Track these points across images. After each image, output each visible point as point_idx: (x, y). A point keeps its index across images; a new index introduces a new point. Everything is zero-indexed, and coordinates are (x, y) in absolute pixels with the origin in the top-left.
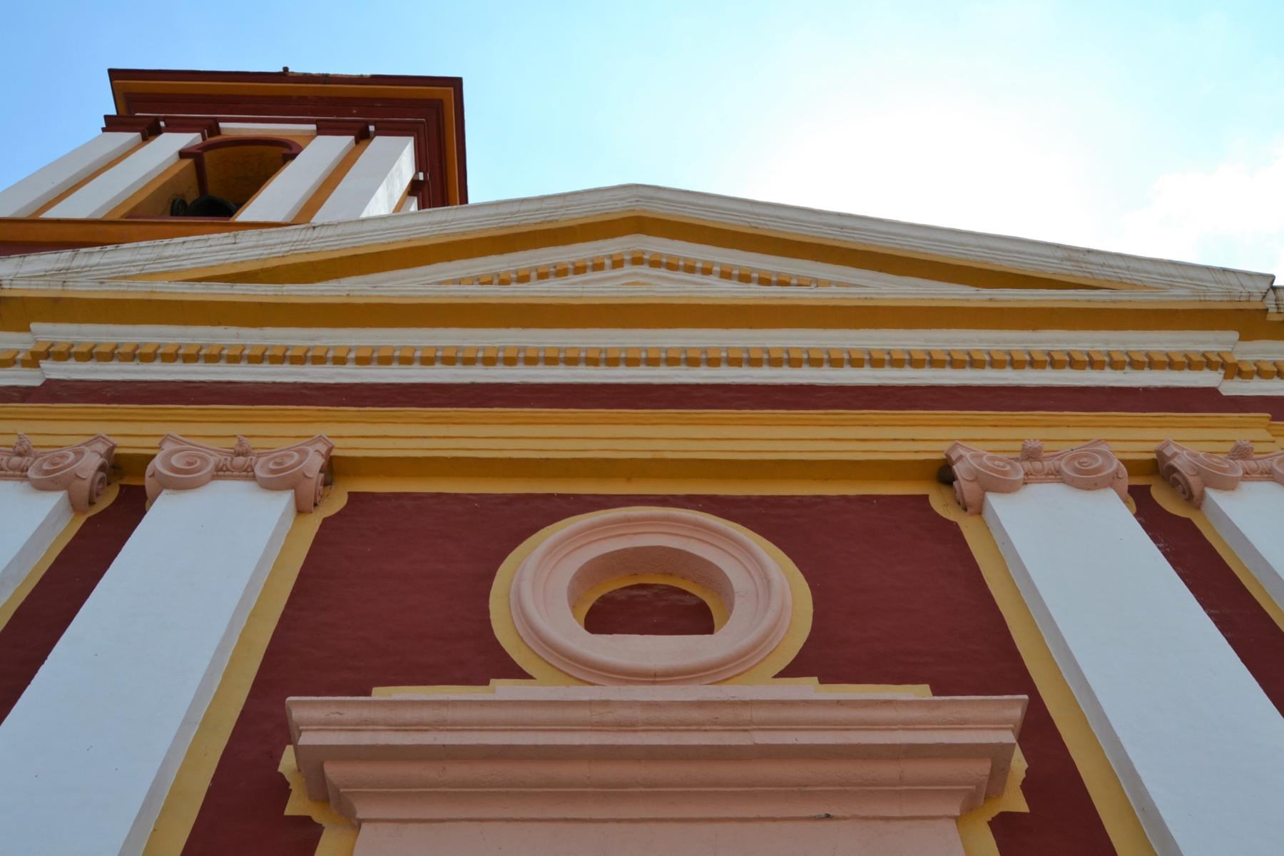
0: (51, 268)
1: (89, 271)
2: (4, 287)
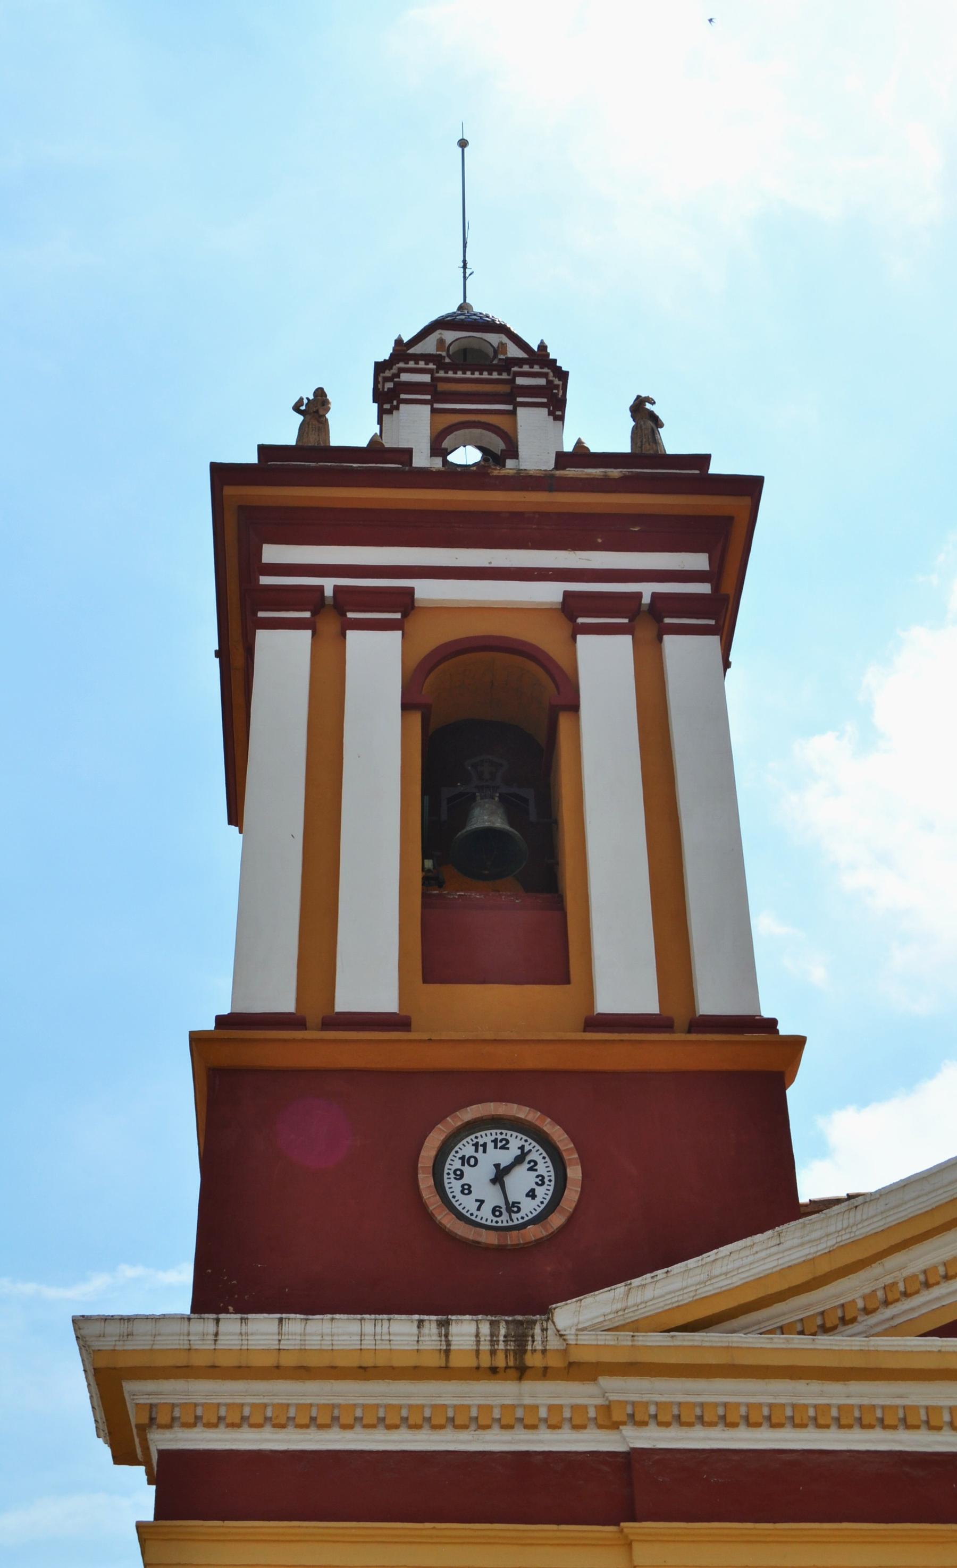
0: (608, 1311)
2: (570, 1342)
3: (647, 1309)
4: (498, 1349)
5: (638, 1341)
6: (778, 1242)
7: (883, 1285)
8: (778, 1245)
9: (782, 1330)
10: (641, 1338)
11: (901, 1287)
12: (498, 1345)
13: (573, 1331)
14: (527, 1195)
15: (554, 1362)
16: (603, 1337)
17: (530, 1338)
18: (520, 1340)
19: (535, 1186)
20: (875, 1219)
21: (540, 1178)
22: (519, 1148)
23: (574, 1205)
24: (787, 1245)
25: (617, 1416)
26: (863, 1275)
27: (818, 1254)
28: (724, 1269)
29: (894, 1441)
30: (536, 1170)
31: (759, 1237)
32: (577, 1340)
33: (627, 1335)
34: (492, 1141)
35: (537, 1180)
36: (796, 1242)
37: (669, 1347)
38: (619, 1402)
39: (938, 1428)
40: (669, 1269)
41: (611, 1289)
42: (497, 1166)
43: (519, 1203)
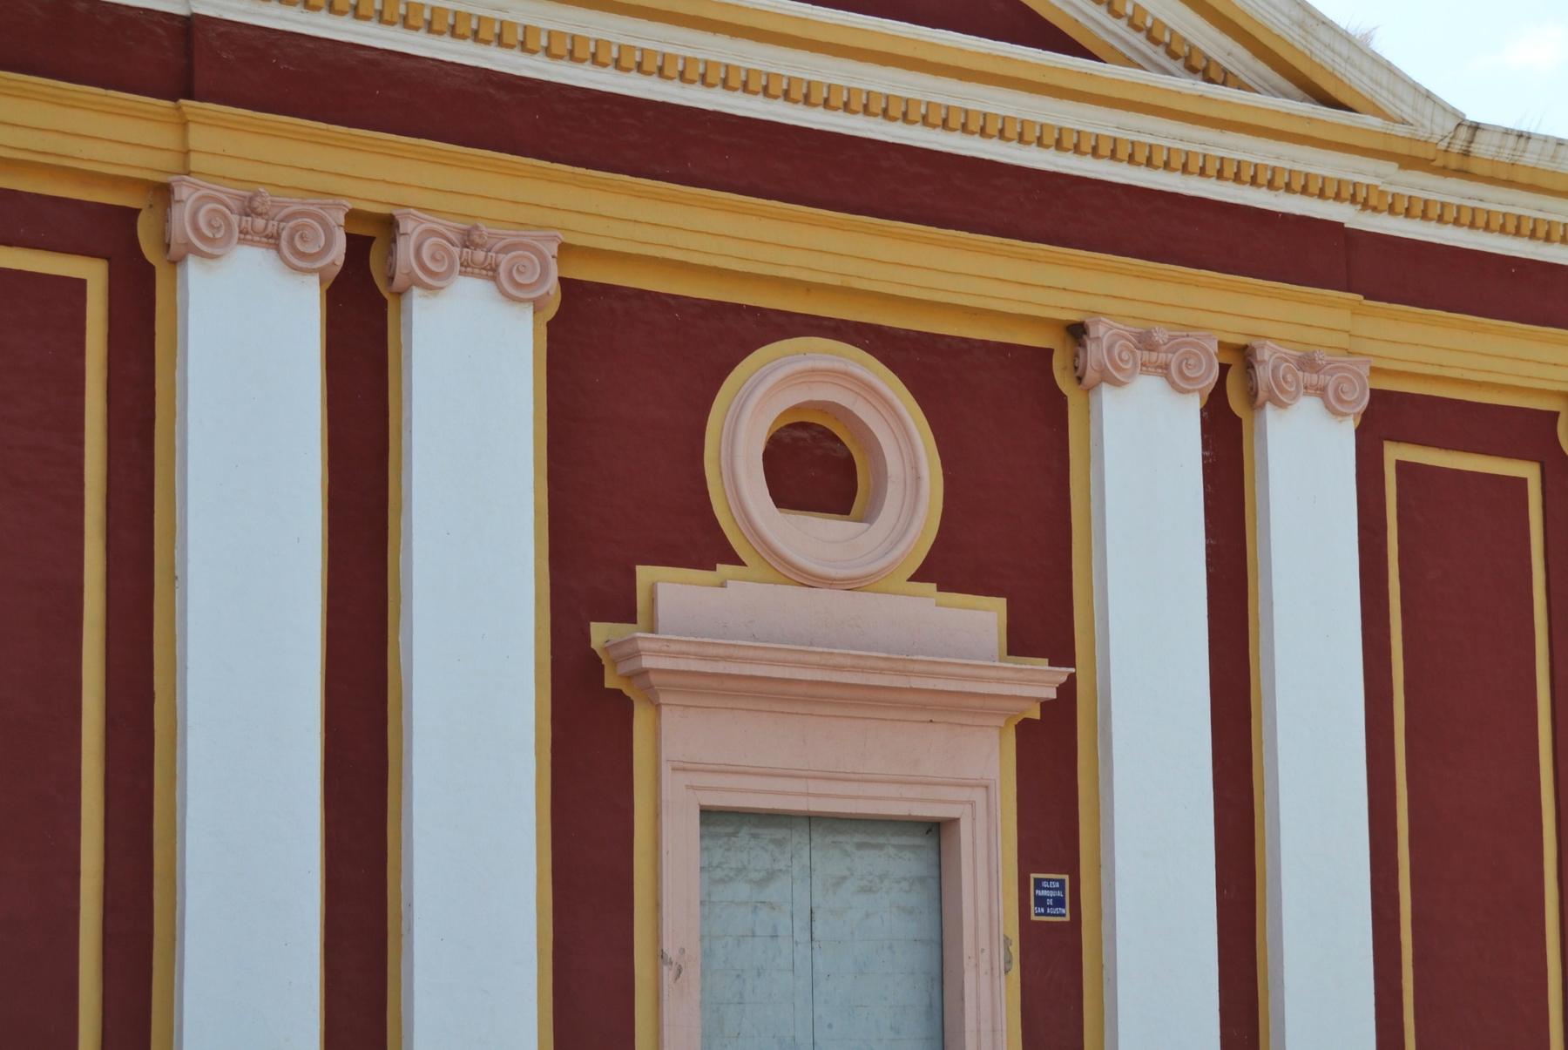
29: (483, 57)
39: (533, 52)
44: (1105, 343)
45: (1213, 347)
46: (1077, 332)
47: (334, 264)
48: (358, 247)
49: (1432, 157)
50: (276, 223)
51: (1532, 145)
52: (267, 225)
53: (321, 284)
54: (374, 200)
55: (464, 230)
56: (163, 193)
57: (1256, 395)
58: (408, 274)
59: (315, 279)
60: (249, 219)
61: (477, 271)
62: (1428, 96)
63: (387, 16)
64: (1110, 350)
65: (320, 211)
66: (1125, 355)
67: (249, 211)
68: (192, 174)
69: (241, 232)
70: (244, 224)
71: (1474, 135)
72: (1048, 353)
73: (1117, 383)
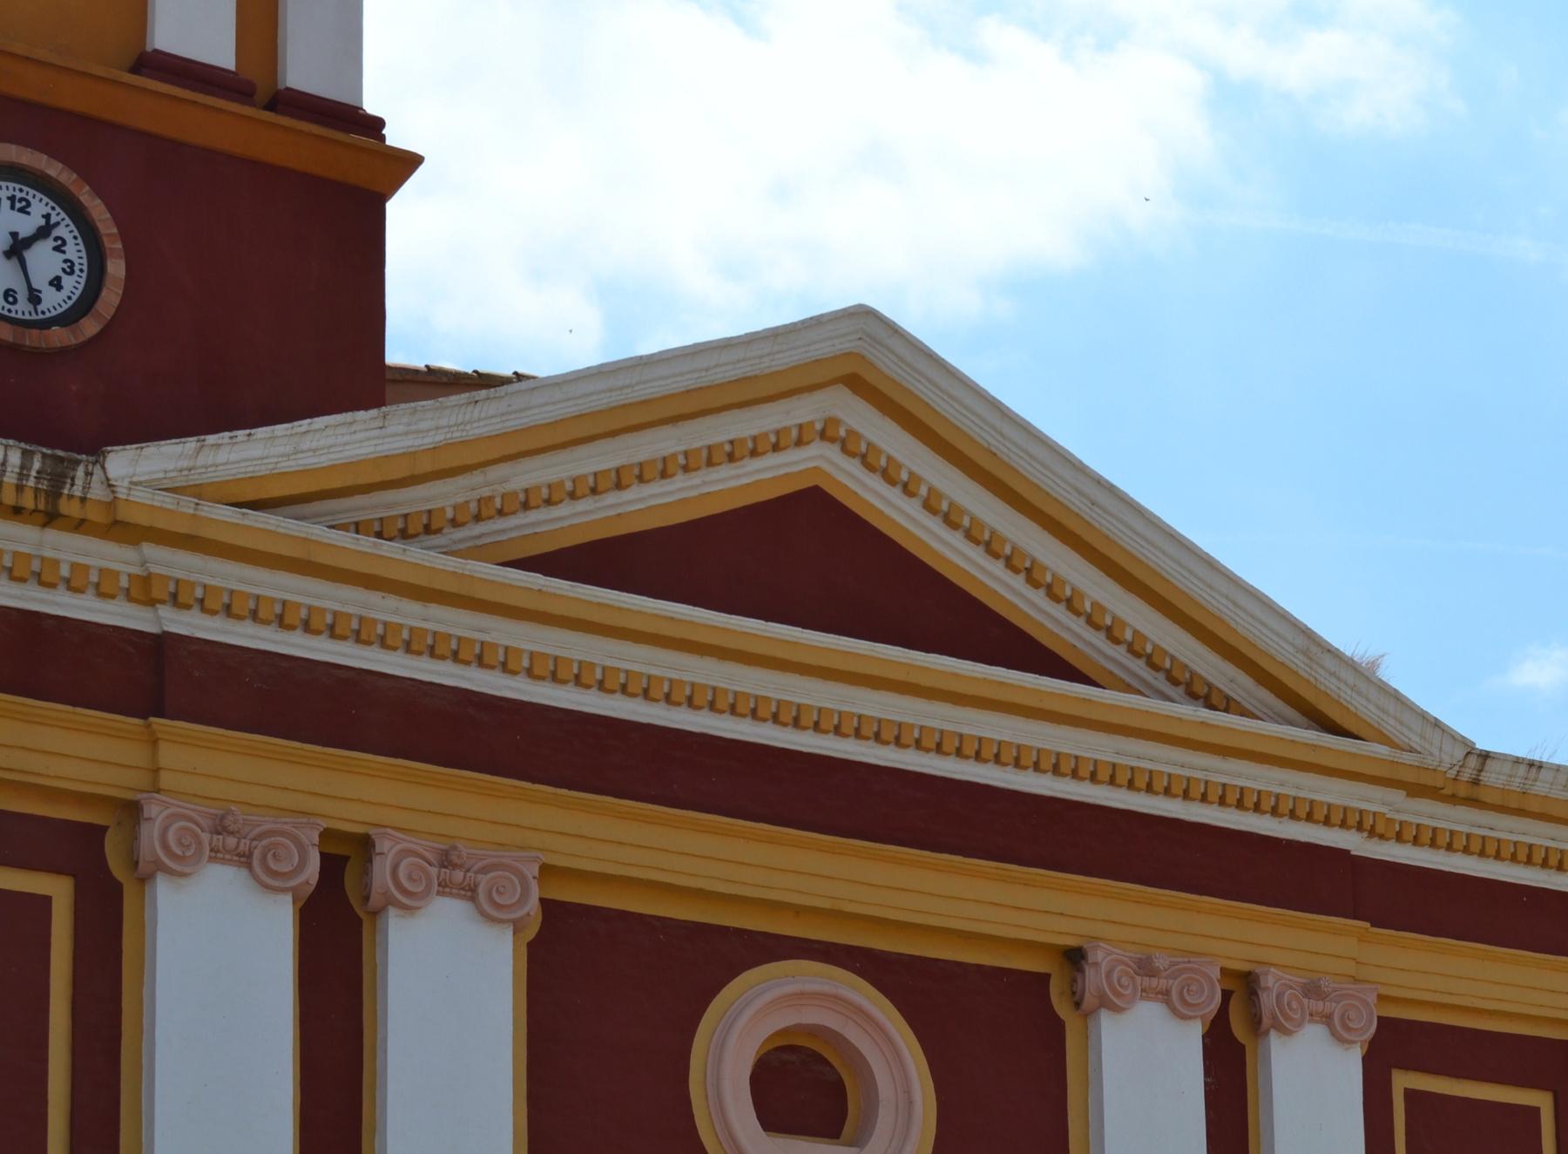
0: (171, 467)
1: (215, 471)
2: (120, 496)
3: (216, 474)
4: (26, 486)
5: (202, 510)
6: (381, 425)
7: (479, 497)
8: (381, 428)
9: (358, 528)
10: (206, 508)
11: (498, 503)
12: (27, 480)
13: (126, 484)
14: (51, 283)
15: (94, 515)
16: (161, 498)
17: (69, 481)
18: (57, 479)
19: (61, 274)
20: (494, 421)
21: (69, 264)
22: (43, 216)
23: (112, 311)
24: (391, 429)
25: (156, 594)
26: (462, 481)
27: (422, 448)
28: (314, 445)
30: (64, 252)
31: (361, 415)
32: (129, 495)
33: (191, 502)
34: (8, 198)
35: (65, 266)
36: (401, 429)
37: (238, 524)
38: (162, 576)
40: (253, 431)
41: (180, 443)
42: (14, 235)
43: (40, 292)
44: (1104, 968)
45: (1215, 974)
46: (1075, 957)
47: (307, 882)
48: (332, 866)
49: (1439, 785)
50: (248, 843)
51: (1543, 774)
52: (238, 843)
53: (294, 903)
54: (350, 818)
55: (443, 850)
56: (132, 811)
57: (1260, 1022)
58: (384, 894)
59: (289, 898)
60: (221, 837)
61: (454, 891)
62: (1437, 724)
63: (364, 636)
64: (1109, 975)
65: (294, 830)
66: (1125, 981)
67: (220, 828)
68: (162, 792)
69: (211, 850)
70: (214, 843)
71: (1483, 764)
72: (1044, 979)
73: (1117, 1009)
